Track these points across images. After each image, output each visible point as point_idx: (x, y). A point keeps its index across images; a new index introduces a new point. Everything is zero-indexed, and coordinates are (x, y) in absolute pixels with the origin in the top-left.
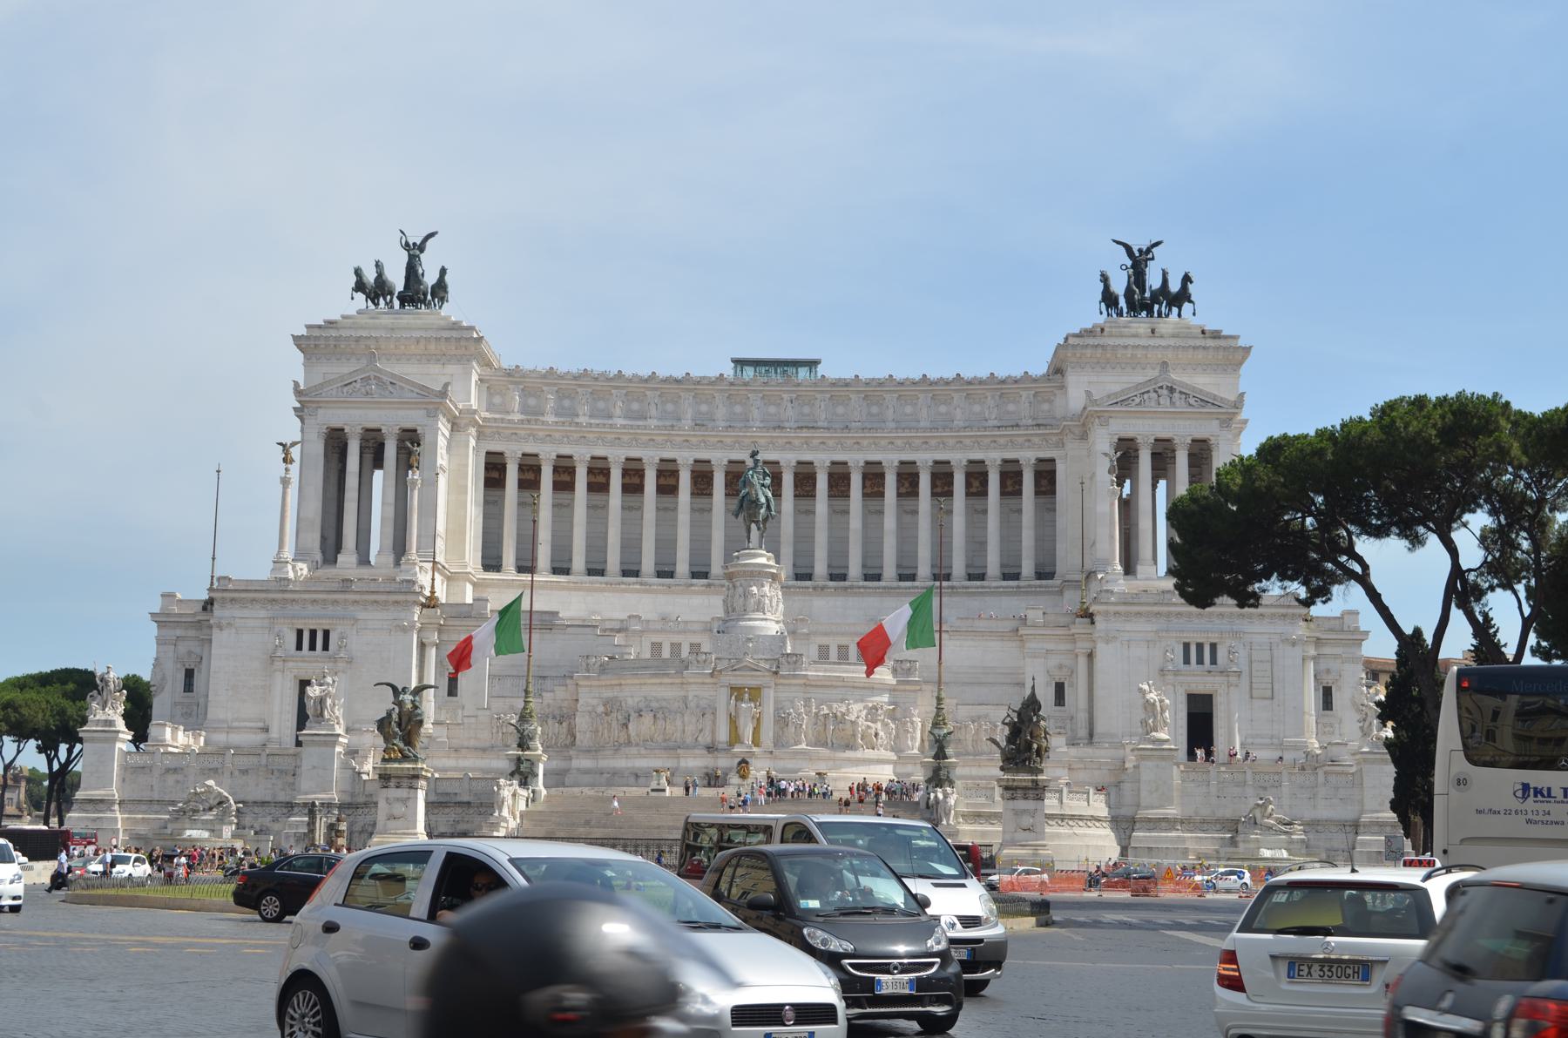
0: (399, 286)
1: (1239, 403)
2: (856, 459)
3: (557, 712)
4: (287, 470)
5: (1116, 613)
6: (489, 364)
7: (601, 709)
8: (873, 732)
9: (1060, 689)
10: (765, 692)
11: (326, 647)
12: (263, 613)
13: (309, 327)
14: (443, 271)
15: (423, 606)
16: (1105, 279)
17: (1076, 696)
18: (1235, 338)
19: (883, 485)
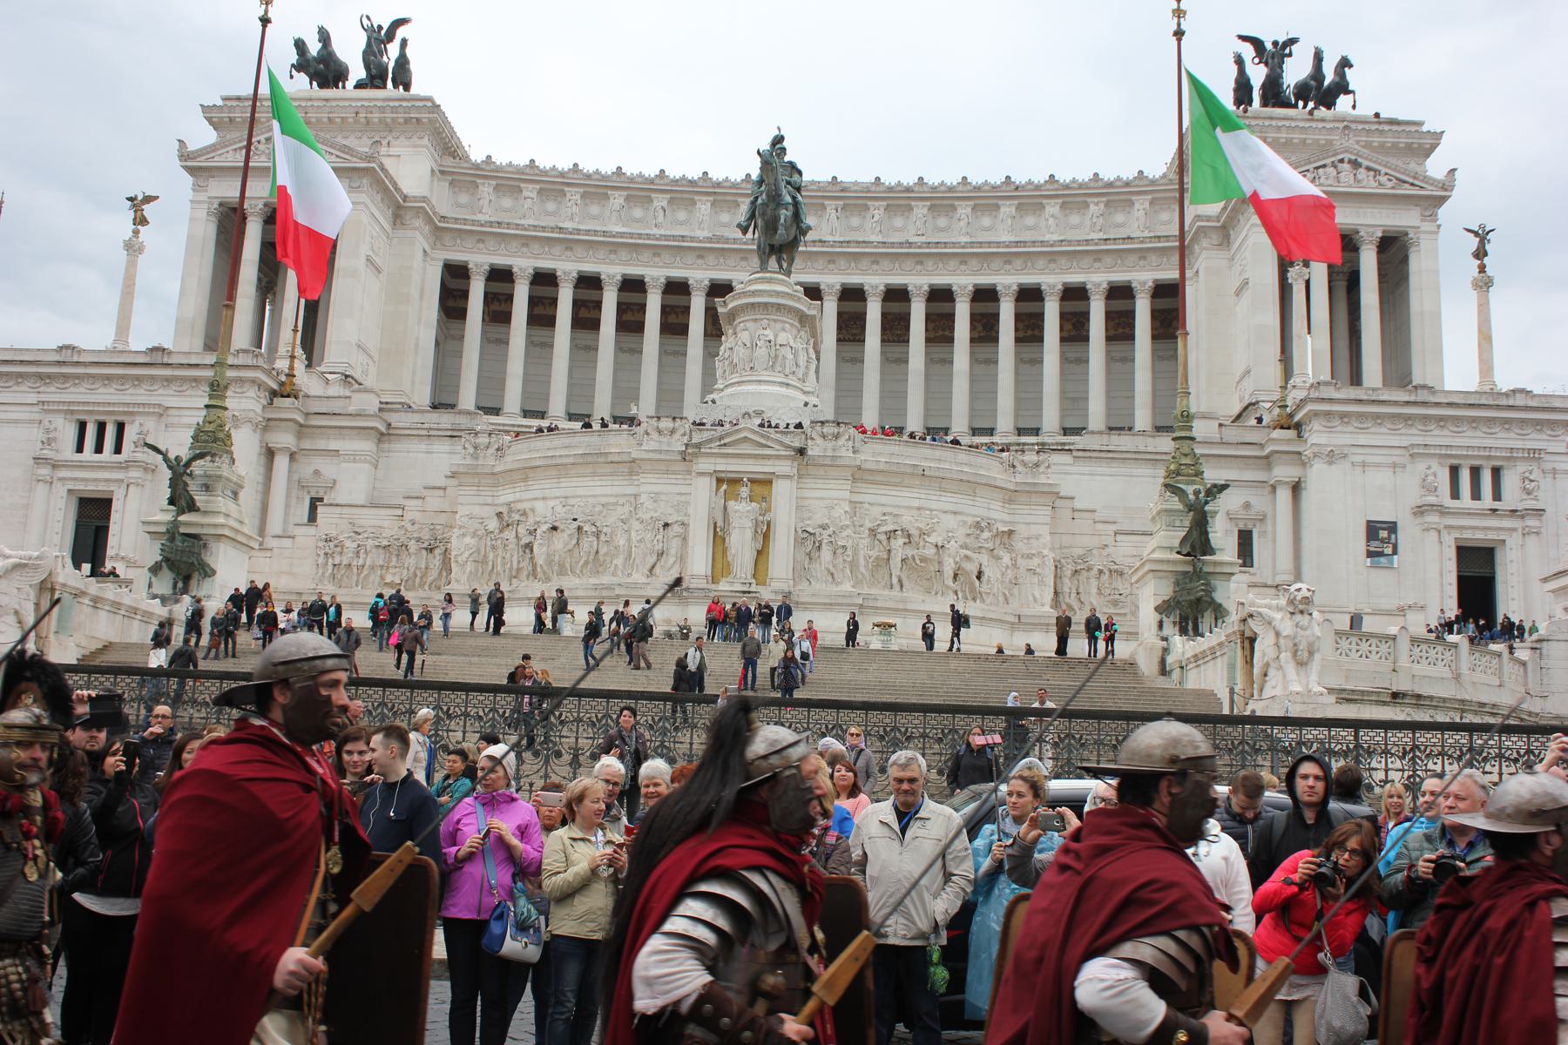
0: (357, 72)
1: (1447, 185)
2: (918, 281)
3: (426, 535)
4: (136, 232)
5: (1343, 416)
6: (454, 155)
7: (493, 524)
8: (972, 568)
9: (1245, 542)
10: (782, 492)
11: (118, 450)
12: (32, 398)
13: (225, 99)
14: (404, 43)
15: (274, 394)
16: (1239, 61)
17: (1272, 552)
18: (1420, 124)
19: (952, 329)
